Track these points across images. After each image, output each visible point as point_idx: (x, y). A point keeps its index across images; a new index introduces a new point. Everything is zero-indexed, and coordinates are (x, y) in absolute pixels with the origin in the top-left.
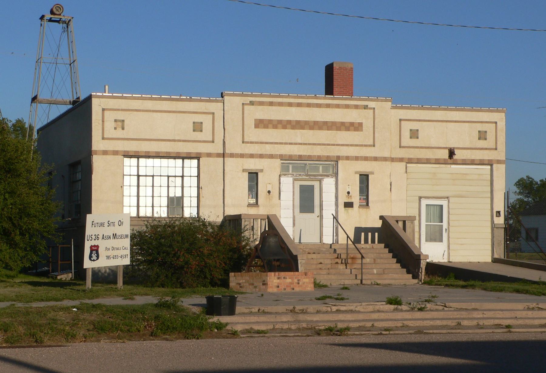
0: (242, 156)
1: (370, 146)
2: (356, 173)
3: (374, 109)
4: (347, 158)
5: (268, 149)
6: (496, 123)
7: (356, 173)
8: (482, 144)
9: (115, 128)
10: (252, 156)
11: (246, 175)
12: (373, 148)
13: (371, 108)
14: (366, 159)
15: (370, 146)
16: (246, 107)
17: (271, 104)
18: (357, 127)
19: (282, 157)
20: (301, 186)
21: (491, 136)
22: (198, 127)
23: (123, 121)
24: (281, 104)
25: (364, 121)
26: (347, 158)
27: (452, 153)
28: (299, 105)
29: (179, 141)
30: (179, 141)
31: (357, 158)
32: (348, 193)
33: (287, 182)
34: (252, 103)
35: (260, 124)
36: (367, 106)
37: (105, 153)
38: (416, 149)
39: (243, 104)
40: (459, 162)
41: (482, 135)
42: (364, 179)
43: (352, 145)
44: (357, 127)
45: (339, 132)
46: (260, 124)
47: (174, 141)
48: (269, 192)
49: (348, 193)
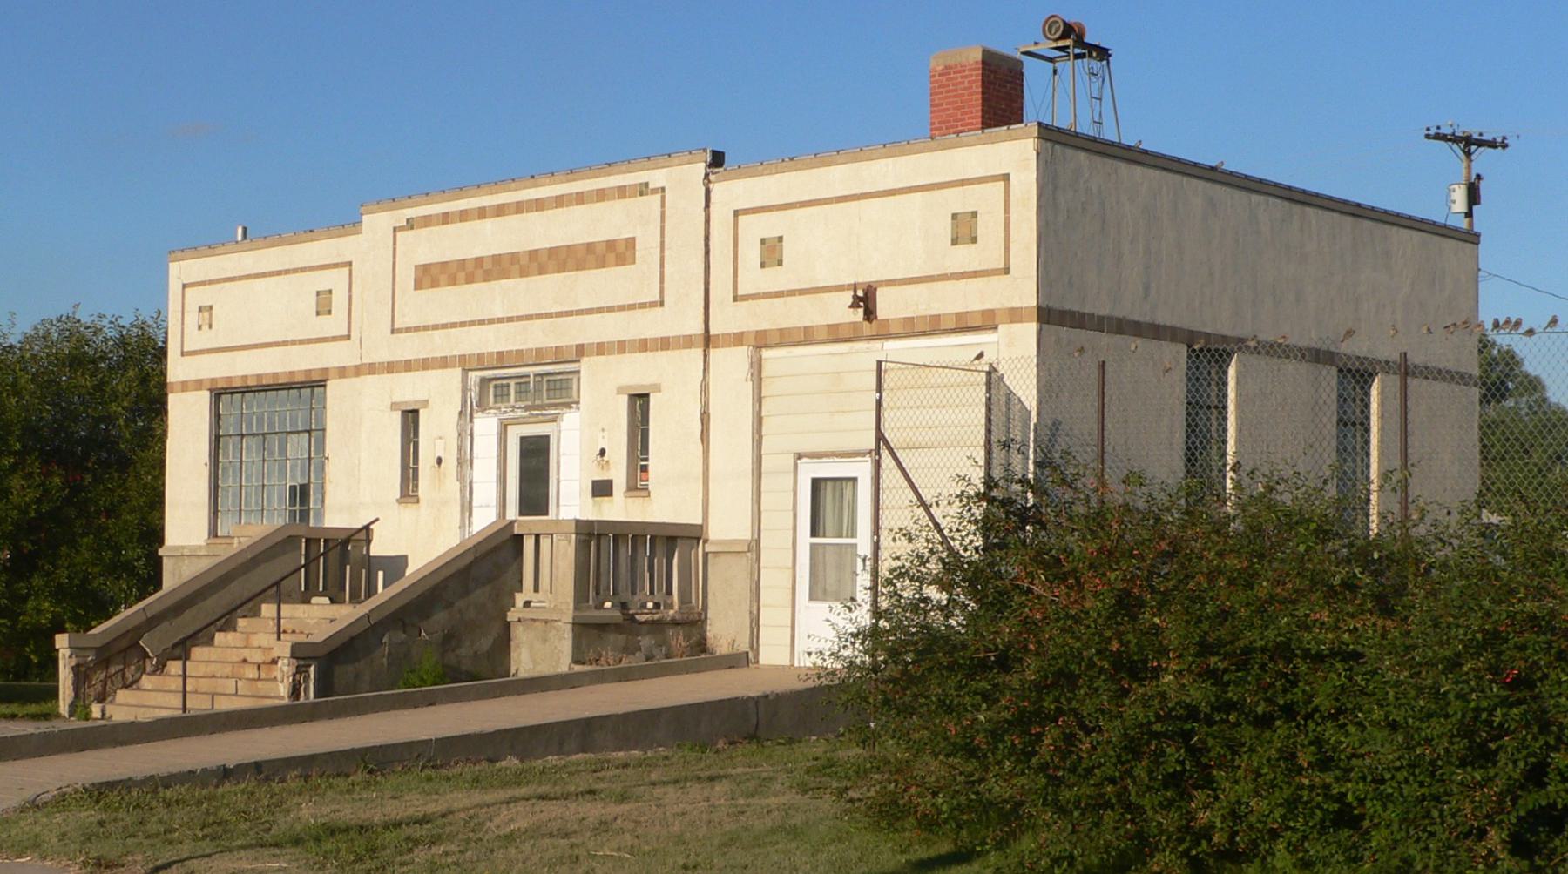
0: (390, 368)
1: (653, 305)
2: (620, 391)
3: (663, 189)
4: (601, 349)
5: (439, 344)
6: (1006, 178)
7: (620, 391)
8: (966, 256)
9: (200, 327)
10: (408, 366)
11: (397, 416)
12: (659, 309)
13: (655, 191)
14: (644, 345)
15: (653, 305)
16: (399, 234)
17: (446, 218)
18: (618, 252)
19: (465, 363)
20: (523, 439)
21: (989, 228)
22: (324, 305)
23: (211, 307)
24: (464, 216)
25: (637, 233)
26: (601, 349)
27: (866, 300)
28: (500, 210)
29: (293, 342)
30: (293, 342)
31: (622, 347)
32: (602, 452)
33: (486, 426)
34: (411, 224)
35: (428, 276)
36: (647, 184)
37: (185, 386)
38: (776, 301)
39: (395, 229)
40: (893, 330)
41: (964, 229)
42: (640, 402)
43: (610, 309)
44: (618, 252)
45: (580, 273)
46: (428, 276)
47: (285, 343)
48: (439, 461)
49: (602, 452)
